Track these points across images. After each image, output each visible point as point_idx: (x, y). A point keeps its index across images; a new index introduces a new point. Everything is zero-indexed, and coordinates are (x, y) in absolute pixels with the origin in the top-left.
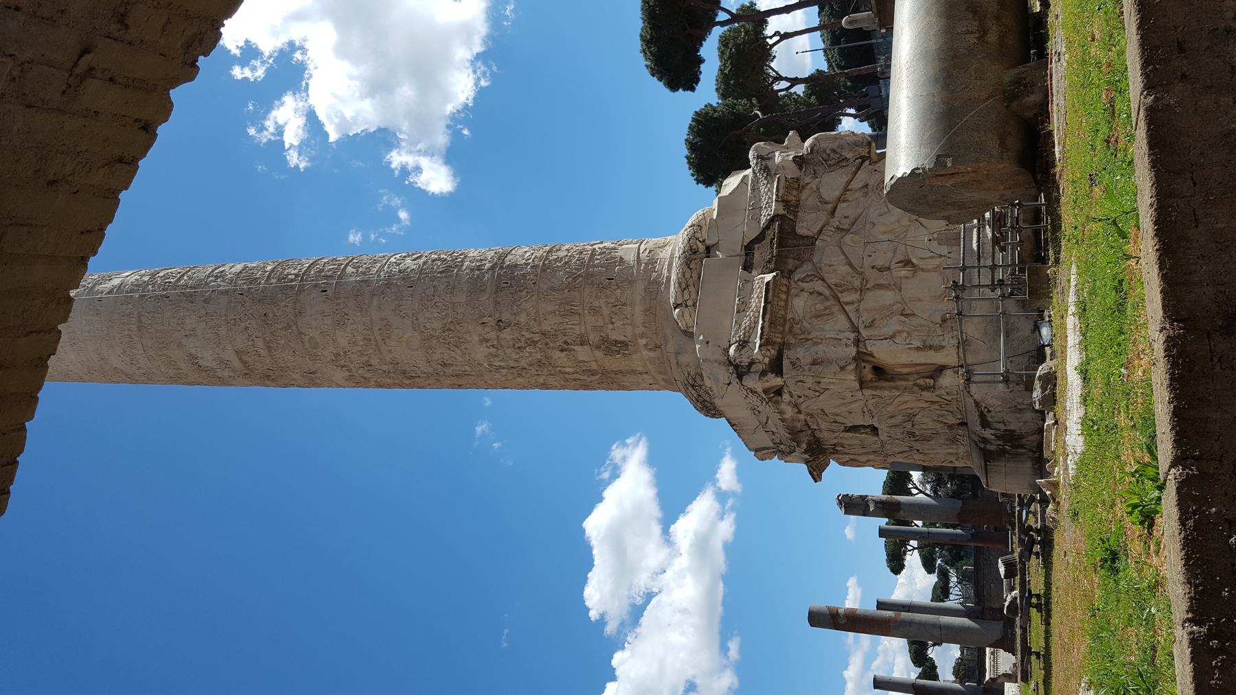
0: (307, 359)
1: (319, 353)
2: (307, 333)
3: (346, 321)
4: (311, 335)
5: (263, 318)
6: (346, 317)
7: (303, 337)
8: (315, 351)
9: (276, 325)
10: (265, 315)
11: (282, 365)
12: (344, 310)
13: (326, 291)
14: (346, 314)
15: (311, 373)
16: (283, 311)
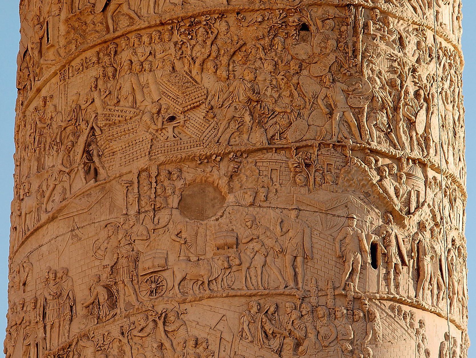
0: (142, 163)
1: (163, 216)
2: (236, 183)
3: (275, 343)
4: (230, 198)
5: (293, 19)
6: (289, 342)
7: (226, 167)
8: (174, 201)
9: (268, 67)
10: (305, 27)
11: (125, 56)
12: (312, 336)
13: (375, 265)
14: (298, 345)
15: (87, 152)
16: (316, 97)
